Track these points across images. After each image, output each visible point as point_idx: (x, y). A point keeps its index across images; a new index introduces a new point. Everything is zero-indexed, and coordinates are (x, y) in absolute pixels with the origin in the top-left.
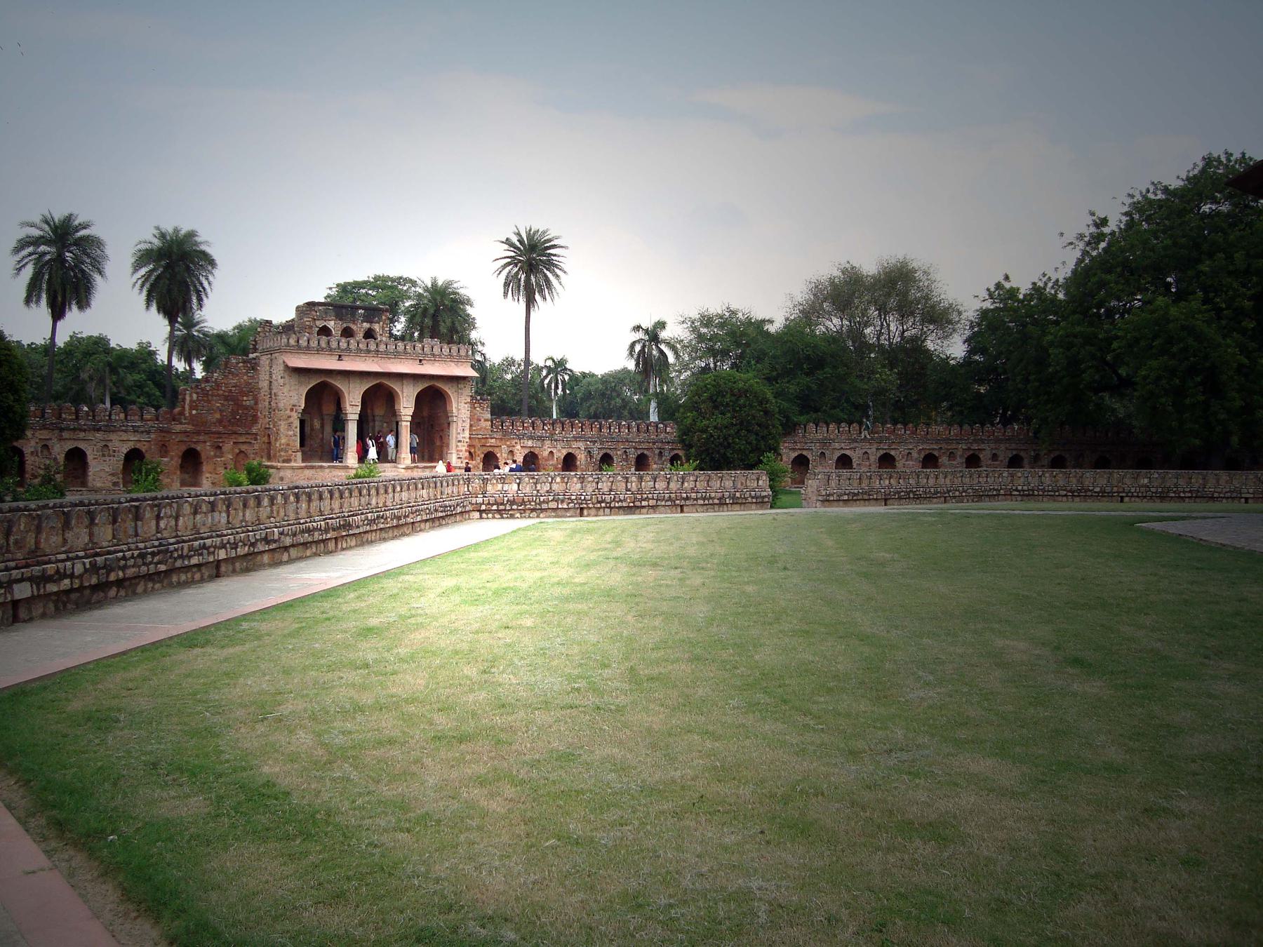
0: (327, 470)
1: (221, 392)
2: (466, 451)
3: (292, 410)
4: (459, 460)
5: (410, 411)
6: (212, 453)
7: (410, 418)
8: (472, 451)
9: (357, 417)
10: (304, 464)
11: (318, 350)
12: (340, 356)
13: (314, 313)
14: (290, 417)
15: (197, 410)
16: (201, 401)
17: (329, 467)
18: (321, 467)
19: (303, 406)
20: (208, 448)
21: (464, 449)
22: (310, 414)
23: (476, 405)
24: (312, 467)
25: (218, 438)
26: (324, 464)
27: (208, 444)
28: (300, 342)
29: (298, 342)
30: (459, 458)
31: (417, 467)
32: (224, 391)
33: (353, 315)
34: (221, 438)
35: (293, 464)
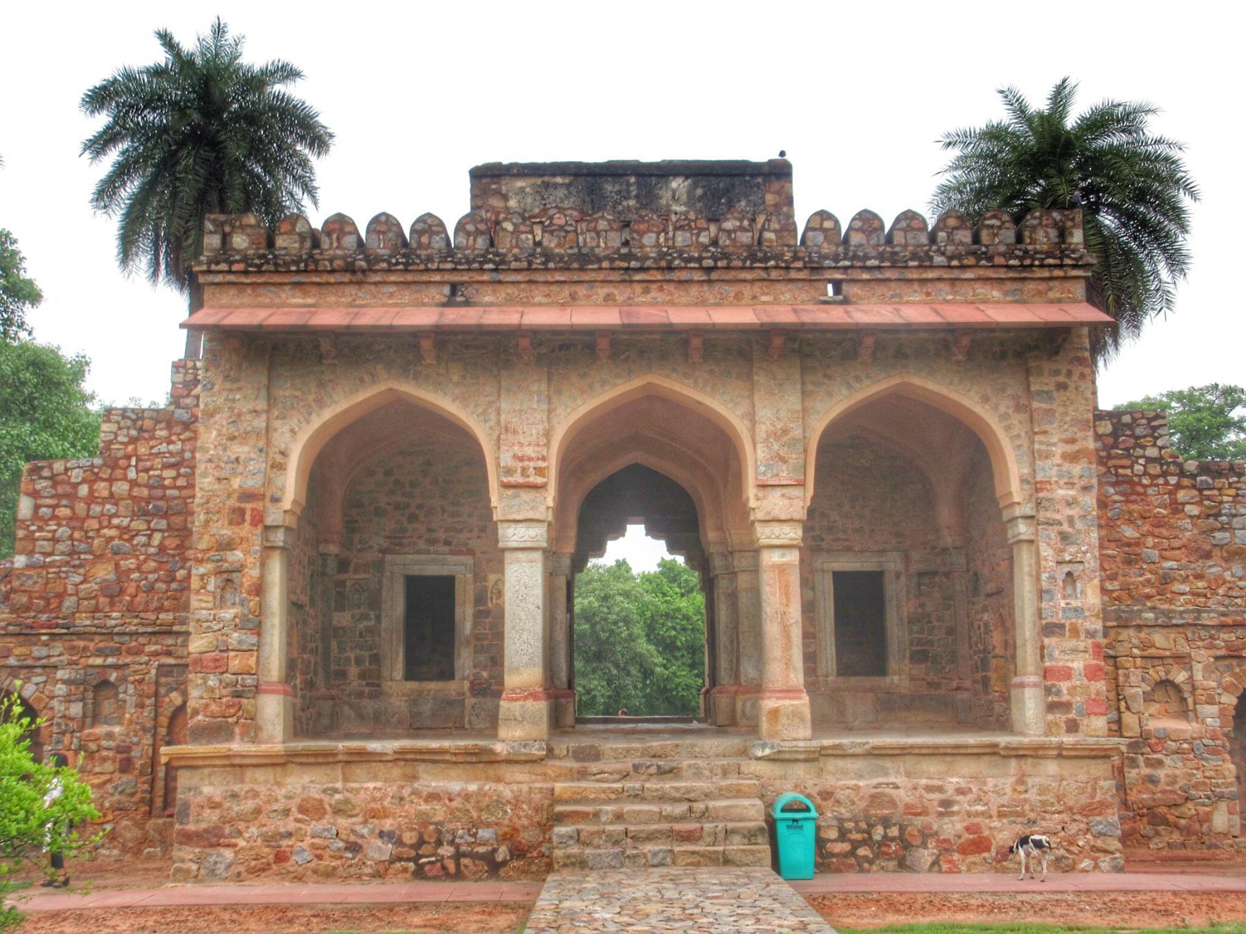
0: (396, 771)
1: (121, 488)
2: (1092, 673)
3: (237, 516)
4: (1060, 717)
5: (794, 503)
6: (76, 709)
7: (794, 533)
8: (1180, 677)
9: (536, 534)
10: (278, 747)
11: (350, 268)
12: (454, 287)
13: (496, 202)
14: (229, 546)
15: (30, 553)
16: (46, 522)
17: (401, 757)
18: (363, 757)
19: (287, 504)
20: (61, 689)
21: (1078, 665)
22: (470, 552)
23: (1181, 496)
24: (323, 759)
25: (100, 652)
26: (374, 746)
27: (60, 674)
28: (280, 242)
29: (271, 244)
30: (1051, 707)
31: (839, 753)
32: (134, 483)
33: (648, 199)
34: (117, 652)
35: (236, 746)
